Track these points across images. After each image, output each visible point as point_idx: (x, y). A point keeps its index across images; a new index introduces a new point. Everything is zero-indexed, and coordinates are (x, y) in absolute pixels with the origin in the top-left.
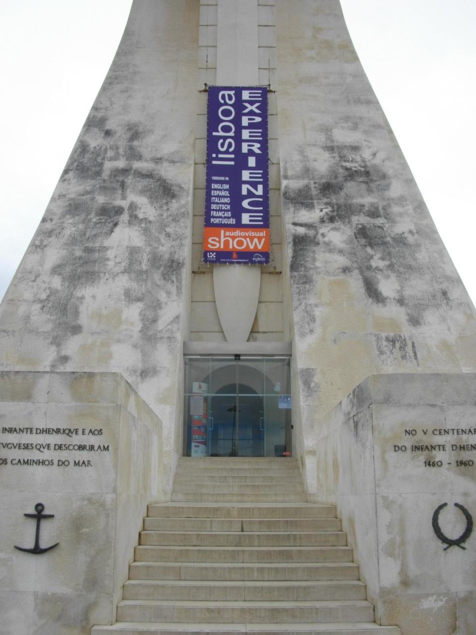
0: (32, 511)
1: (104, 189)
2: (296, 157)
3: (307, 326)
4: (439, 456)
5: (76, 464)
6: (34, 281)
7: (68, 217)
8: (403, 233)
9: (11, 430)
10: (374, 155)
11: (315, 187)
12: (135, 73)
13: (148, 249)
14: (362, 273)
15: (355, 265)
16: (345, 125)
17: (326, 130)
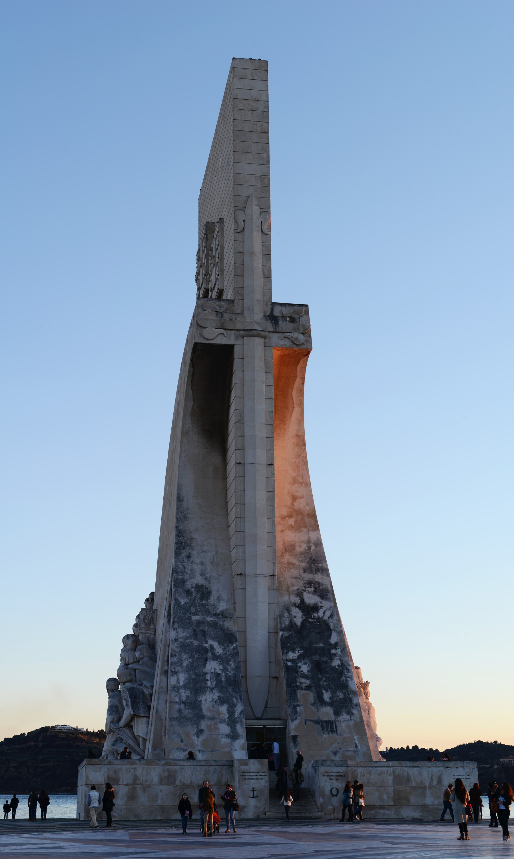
0: (252, 789)
1: (195, 635)
2: (286, 615)
3: (294, 716)
4: (332, 777)
5: (260, 779)
6: (178, 692)
7: (183, 654)
8: (335, 666)
9: (246, 772)
10: (324, 613)
11: (296, 636)
12: (192, 539)
13: (224, 674)
16: (310, 589)
17: (300, 594)
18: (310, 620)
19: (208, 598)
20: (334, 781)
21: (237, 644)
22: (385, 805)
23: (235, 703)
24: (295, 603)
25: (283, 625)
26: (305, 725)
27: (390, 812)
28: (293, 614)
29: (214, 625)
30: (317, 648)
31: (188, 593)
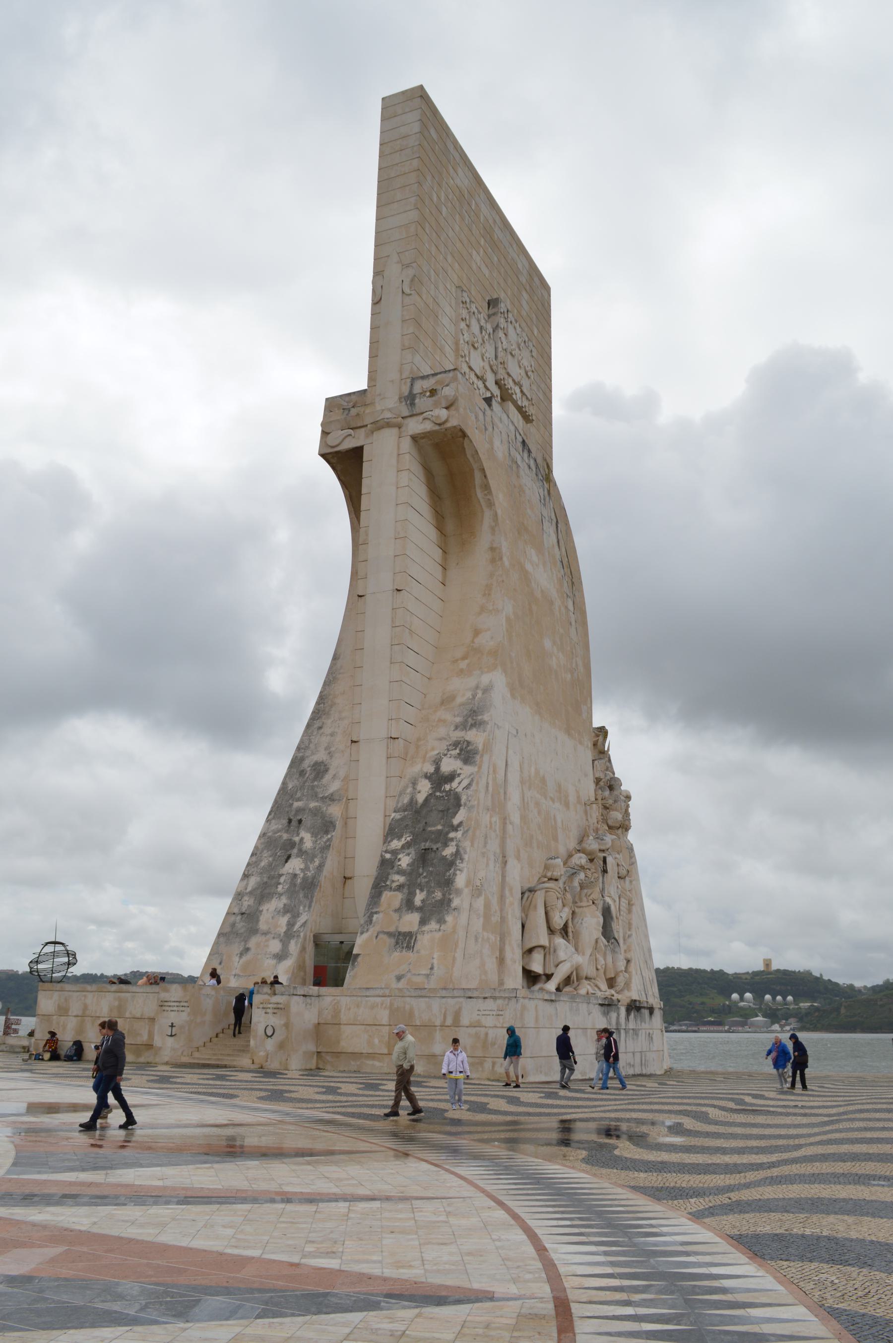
4: (268, 1011)
6: (240, 900)
10: (459, 783)
14: (409, 889)
15: (408, 883)
18: (438, 794)
19: (322, 778)
20: (270, 1015)
21: (333, 834)
22: (374, 1053)
23: (301, 912)
24: (427, 773)
25: (400, 805)
26: (375, 939)
27: (381, 1064)
28: (419, 787)
29: (316, 812)
30: (432, 832)
31: (302, 773)
